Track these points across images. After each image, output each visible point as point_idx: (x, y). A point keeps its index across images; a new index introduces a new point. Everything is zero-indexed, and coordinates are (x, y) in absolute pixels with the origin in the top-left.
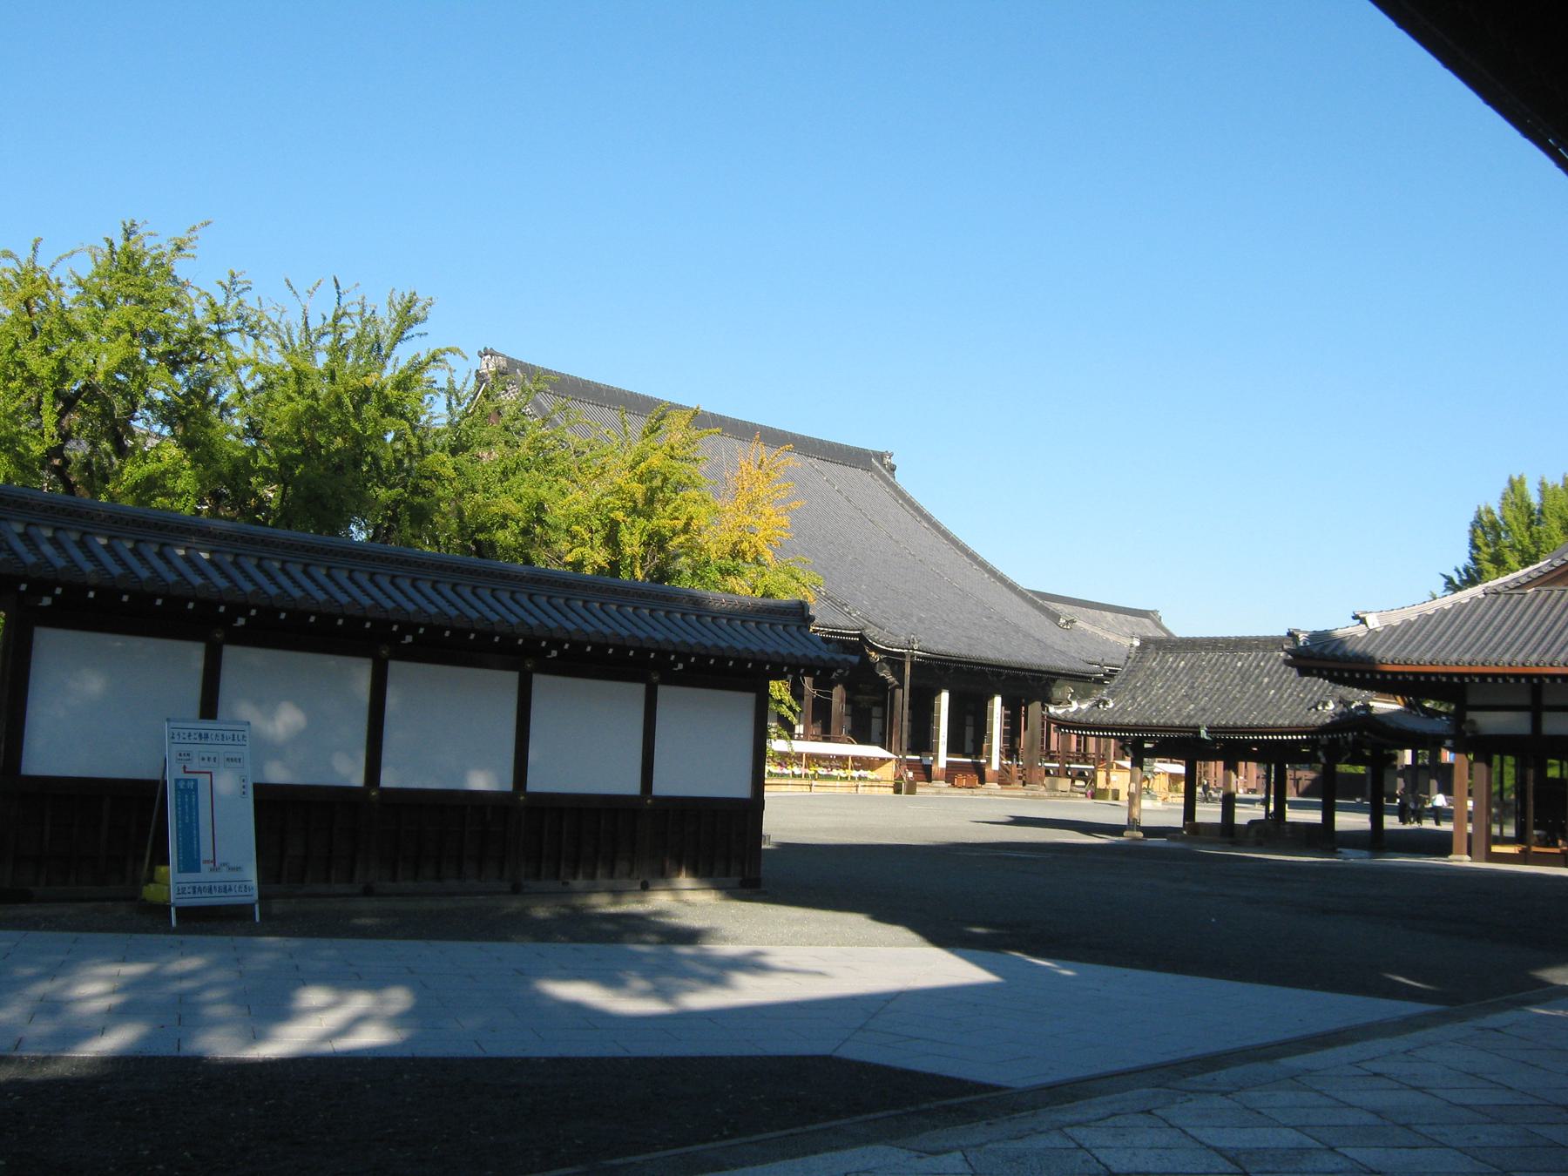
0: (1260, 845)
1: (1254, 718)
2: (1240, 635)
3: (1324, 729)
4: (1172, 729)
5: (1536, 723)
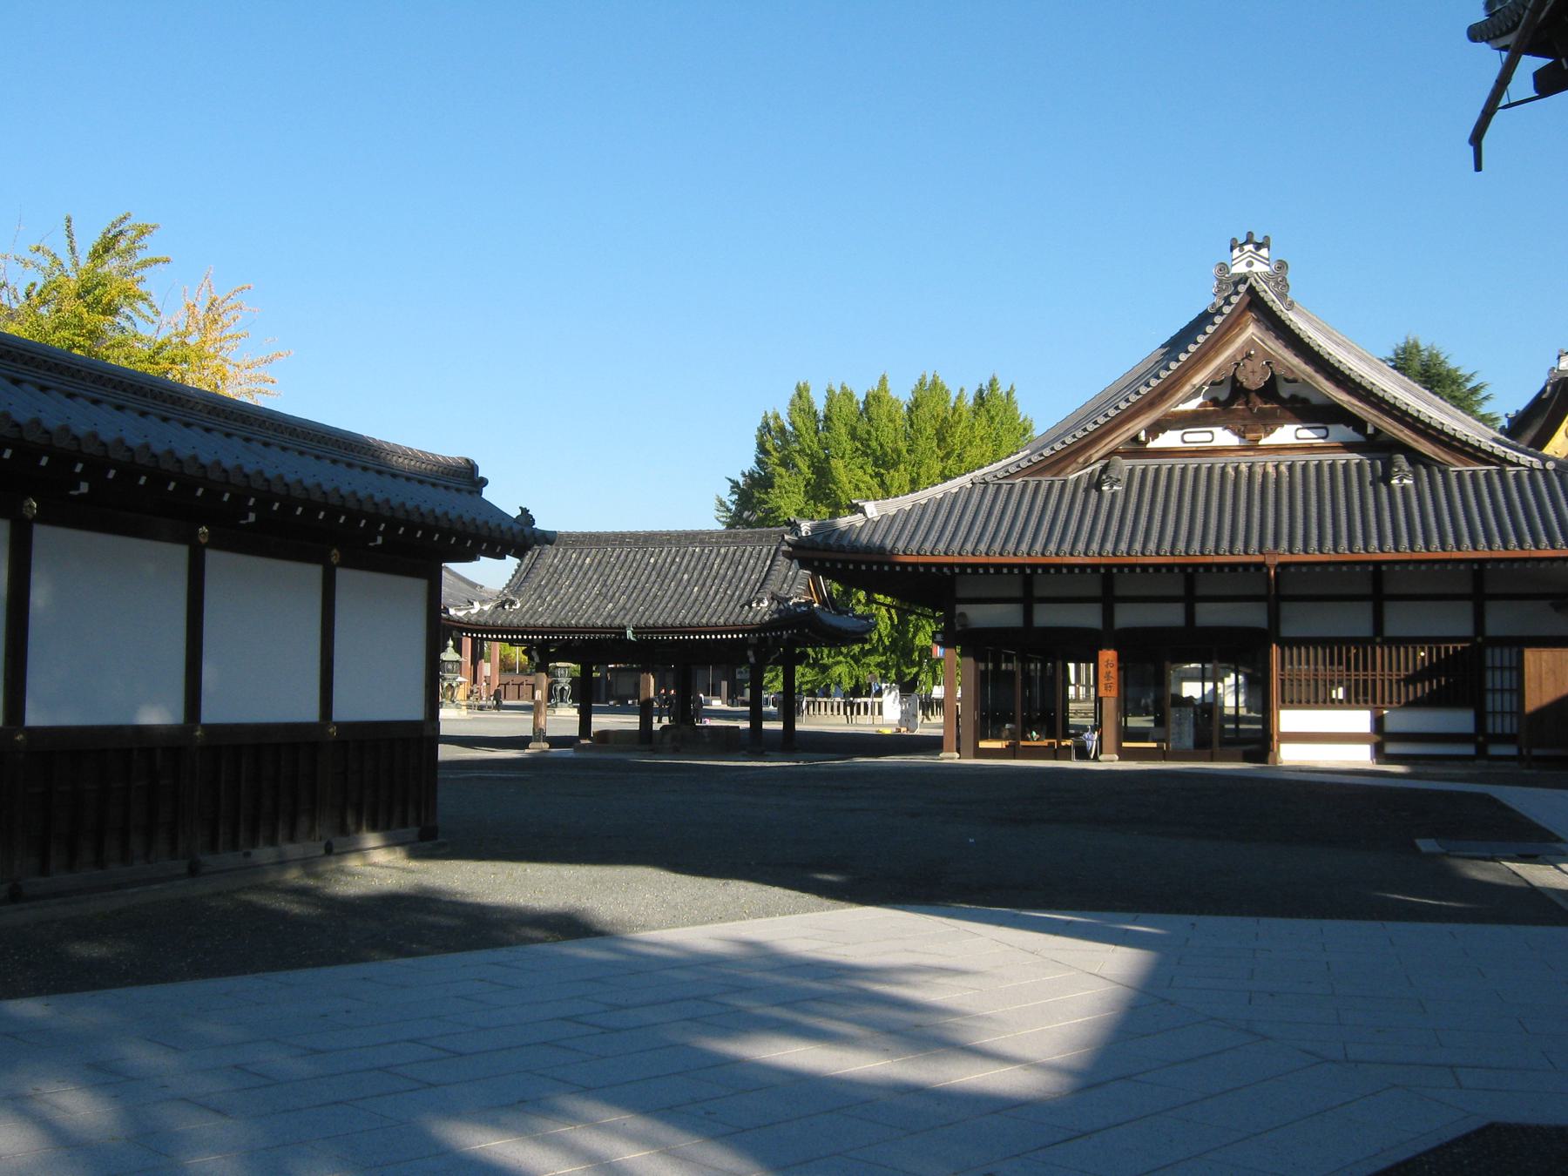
0: (676, 751)
1: (683, 617)
2: (648, 529)
3: (764, 627)
4: (593, 629)
5: (1028, 615)
